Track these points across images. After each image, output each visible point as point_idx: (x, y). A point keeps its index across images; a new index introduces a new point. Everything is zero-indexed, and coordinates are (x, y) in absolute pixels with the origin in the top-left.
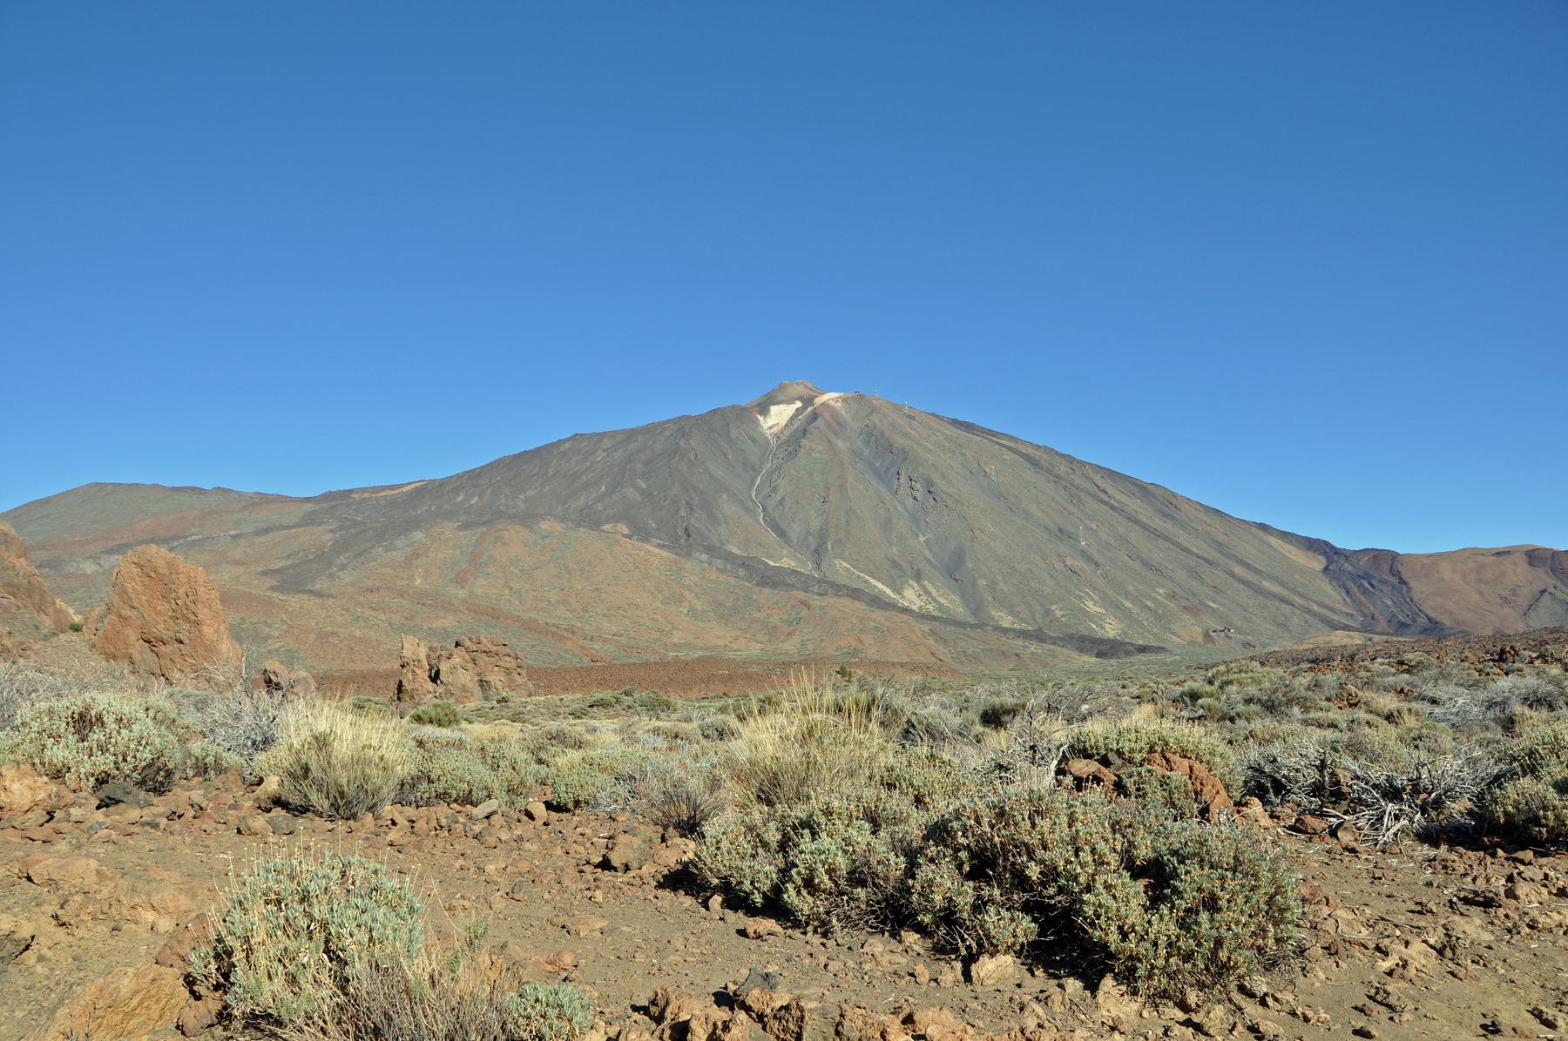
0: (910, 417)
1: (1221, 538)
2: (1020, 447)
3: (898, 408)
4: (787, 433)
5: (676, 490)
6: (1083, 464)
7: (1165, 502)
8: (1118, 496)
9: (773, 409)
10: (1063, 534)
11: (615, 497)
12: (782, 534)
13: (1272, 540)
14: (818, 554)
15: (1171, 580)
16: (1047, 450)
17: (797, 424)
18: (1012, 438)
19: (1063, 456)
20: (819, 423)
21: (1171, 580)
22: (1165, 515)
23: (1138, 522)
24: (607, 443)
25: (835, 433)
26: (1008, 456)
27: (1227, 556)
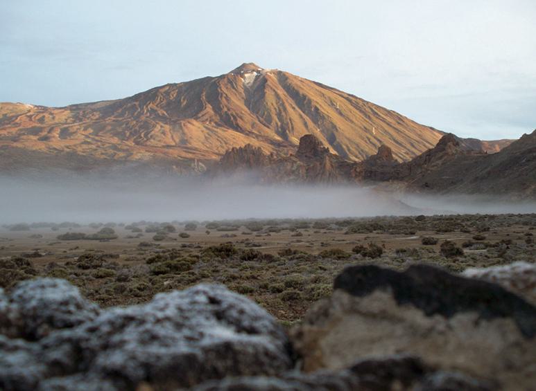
0: (301, 81)
1: (419, 133)
2: (343, 94)
3: (296, 77)
4: (256, 86)
5: (225, 109)
6: (368, 103)
7: (400, 119)
8: (383, 116)
9: (246, 75)
10: (366, 130)
11: (203, 113)
12: (268, 127)
13: (437, 134)
14: (283, 134)
15: (405, 147)
16: (352, 96)
17: (258, 83)
18: (338, 90)
19: (360, 99)
20: (269, 83)
21: (405, 147)
22: (399, 123)
23: (391, 126)
24: (184, 88)
25: (276, 87)
26: (342, 99)
27: (424, 140)
